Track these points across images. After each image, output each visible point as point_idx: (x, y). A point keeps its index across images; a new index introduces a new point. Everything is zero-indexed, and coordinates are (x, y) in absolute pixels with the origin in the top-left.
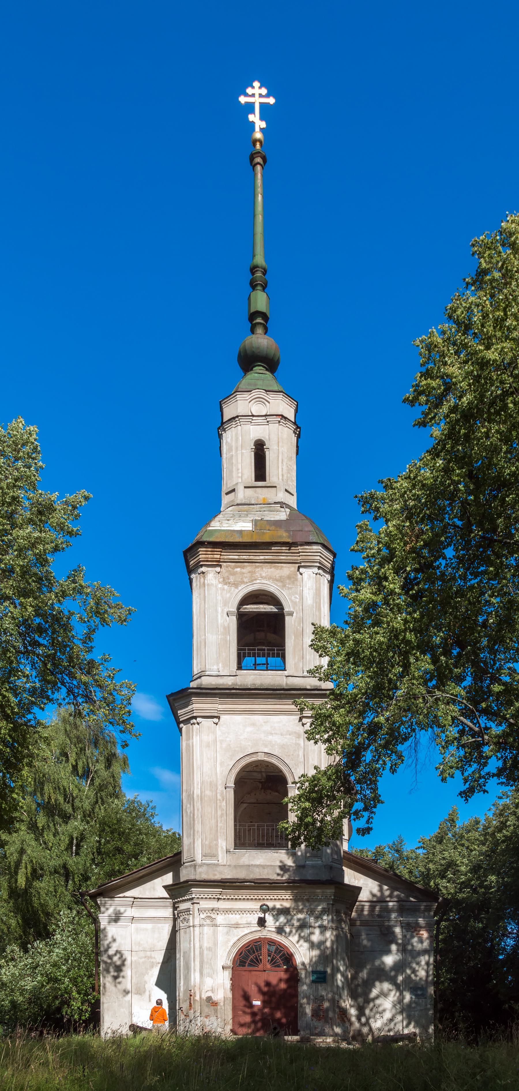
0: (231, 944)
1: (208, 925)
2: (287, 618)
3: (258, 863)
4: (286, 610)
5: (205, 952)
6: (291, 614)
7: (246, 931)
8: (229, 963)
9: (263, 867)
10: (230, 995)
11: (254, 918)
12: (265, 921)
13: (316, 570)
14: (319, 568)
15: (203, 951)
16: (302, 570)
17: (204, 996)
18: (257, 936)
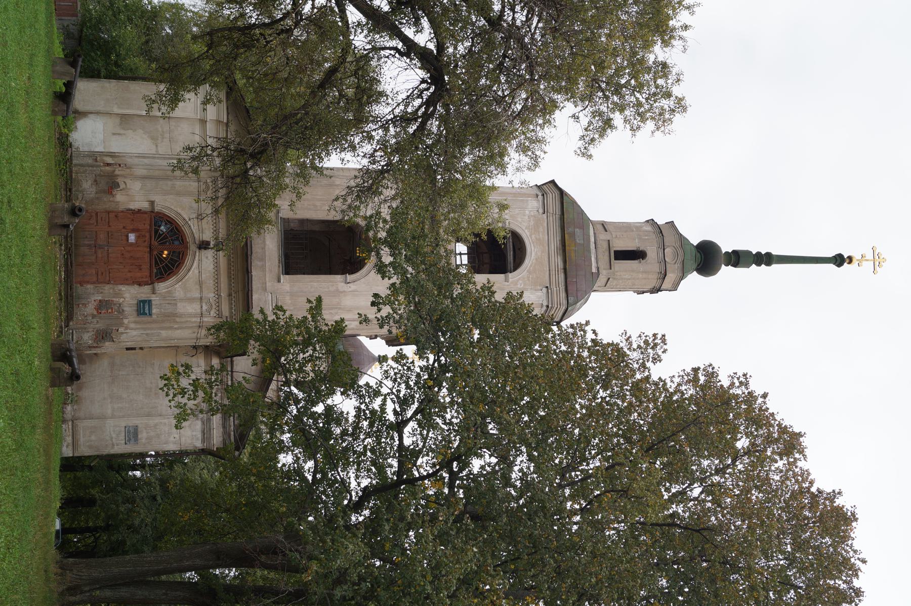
0: (179, 211)
1: (199, 187)
2: (502, 275)
3: (268, 242)
4: (510, 275)
5: (169, 183)
6: (506, 280)
7: (195, 229)
8: (157, 209)
9: (263, 248)
10: (122, 208)
11: (208, 236)
12: (206, 248)
13: (545, 304)
14: (548, 306)
15: (171, 180)
16: (545, 290)
17: (120, 180)
18: (189, 239)
